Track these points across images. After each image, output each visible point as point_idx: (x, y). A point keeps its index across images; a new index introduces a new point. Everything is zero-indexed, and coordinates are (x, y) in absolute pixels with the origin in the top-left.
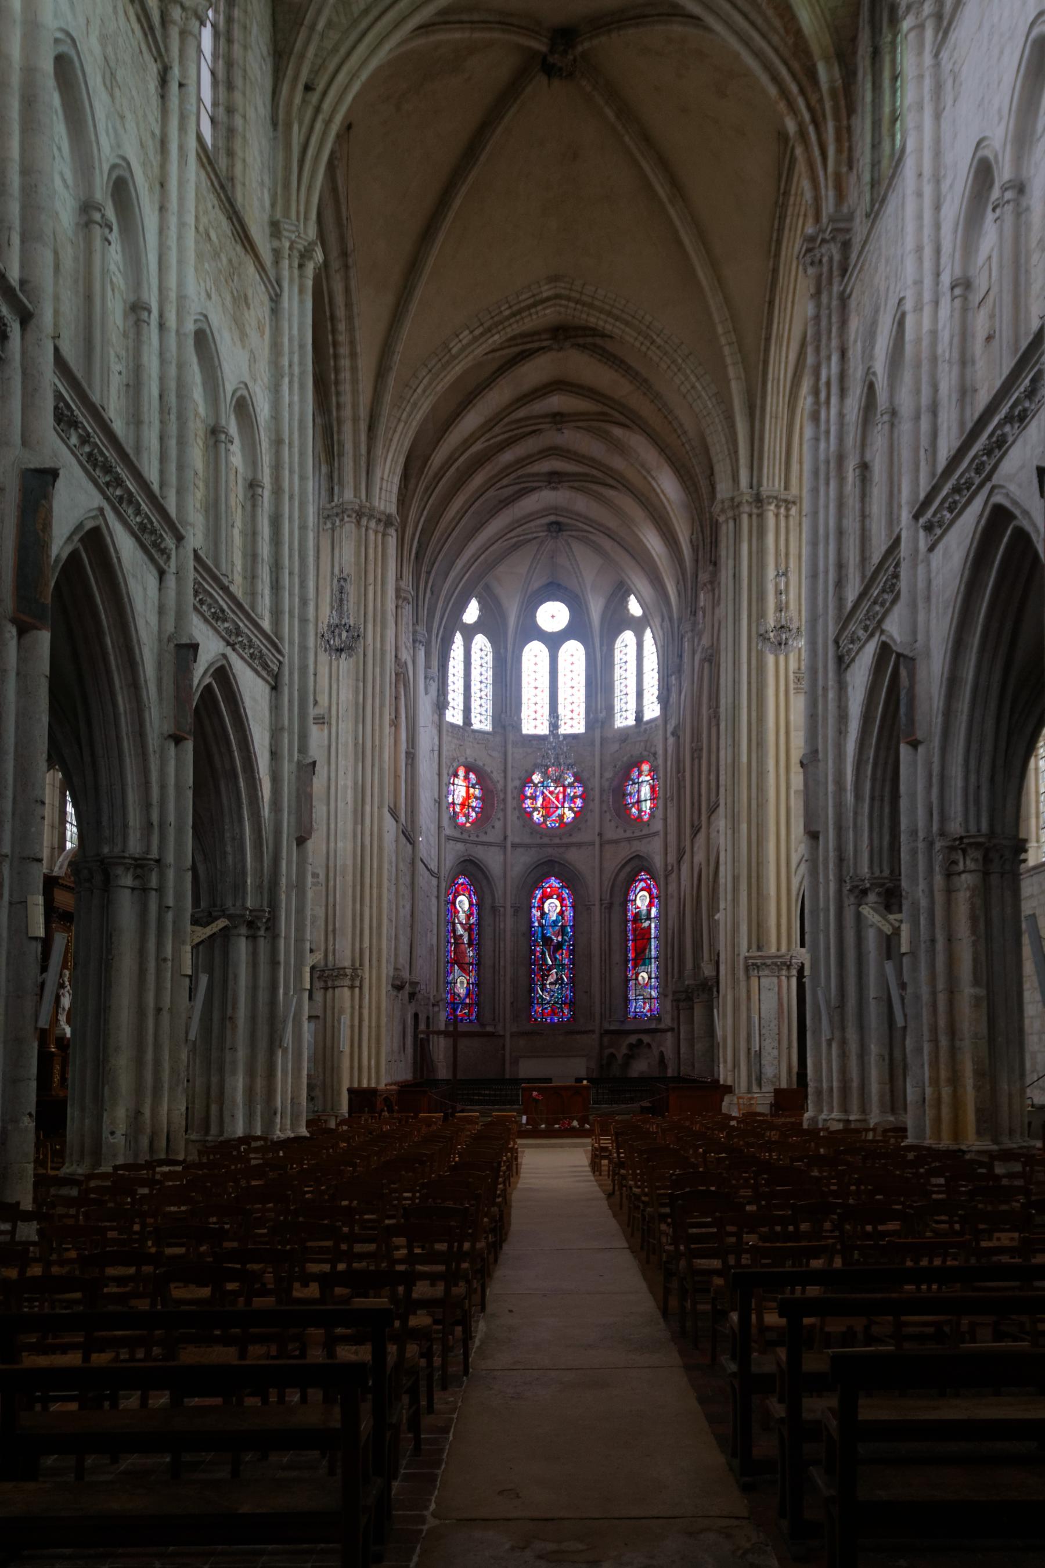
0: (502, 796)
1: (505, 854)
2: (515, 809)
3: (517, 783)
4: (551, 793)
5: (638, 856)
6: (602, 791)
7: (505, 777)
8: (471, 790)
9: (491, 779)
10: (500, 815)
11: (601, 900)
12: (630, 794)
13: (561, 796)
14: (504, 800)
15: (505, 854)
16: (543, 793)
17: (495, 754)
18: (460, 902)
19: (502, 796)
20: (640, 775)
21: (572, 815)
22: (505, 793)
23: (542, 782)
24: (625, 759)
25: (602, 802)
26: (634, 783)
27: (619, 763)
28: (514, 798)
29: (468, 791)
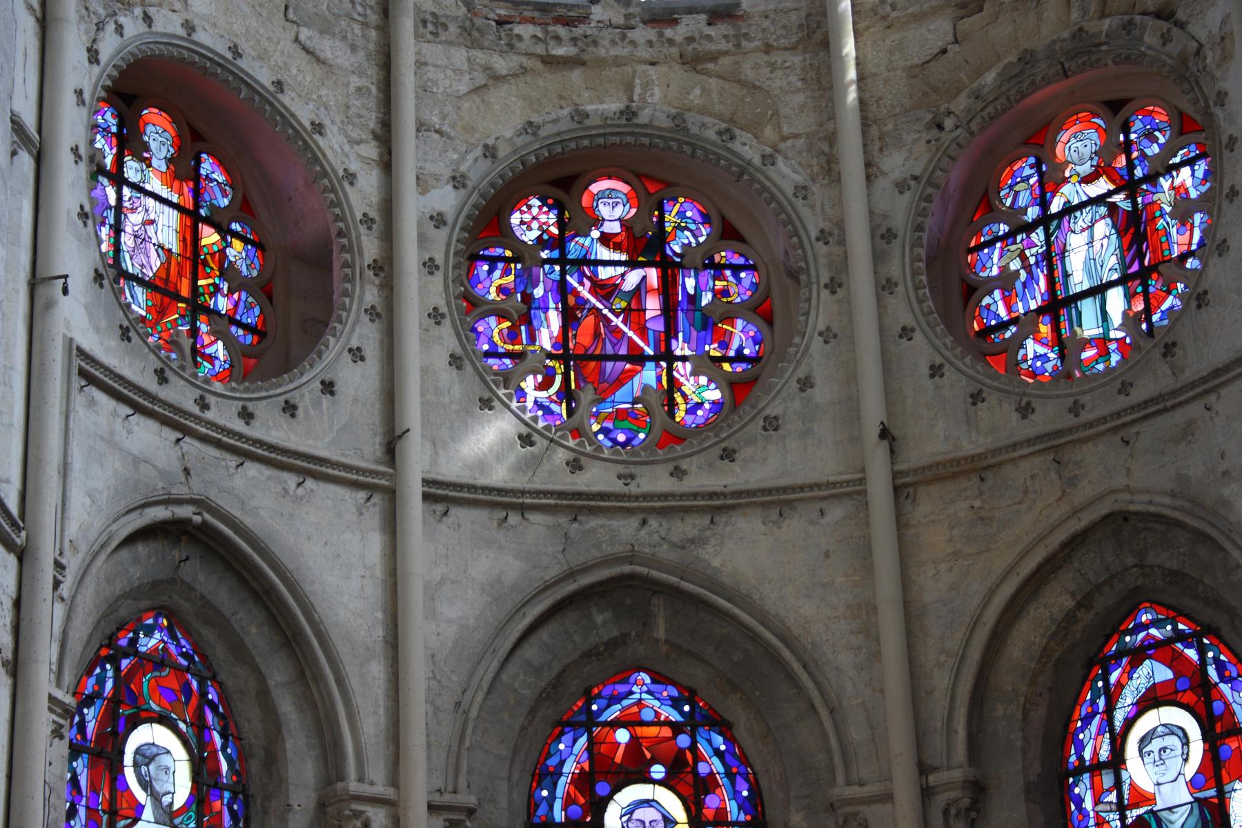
0: (370, 248)
1: (392, 524)
2: (436, 316)
3: (446, 199)
4: (606, 290)
5: (1118, 521)
6: (882, 235)
7: (387, 164)
8: (210, 237)
9: (314, 158)
10: (366, 334)
11: (923, 769)
12: (1006, 281)
13: (653, 305)
14: (386, 269)
15: (392, 524)
16: (562, 289)
17: (328, 47)
18: (147, 755)
19: (370, 248)
20: (1048, 185)
21: (715, 395)
22: (389, 235)
23: (559, 243)
24: (990, 78)
25: (885, 286)
26: (1030, 228)
27: (961, 103)
28: (430, 266)
29: (191, 238)
